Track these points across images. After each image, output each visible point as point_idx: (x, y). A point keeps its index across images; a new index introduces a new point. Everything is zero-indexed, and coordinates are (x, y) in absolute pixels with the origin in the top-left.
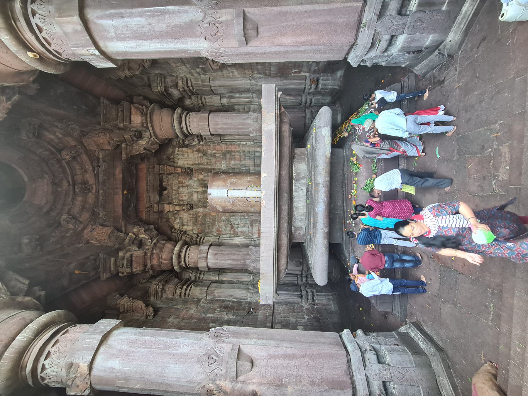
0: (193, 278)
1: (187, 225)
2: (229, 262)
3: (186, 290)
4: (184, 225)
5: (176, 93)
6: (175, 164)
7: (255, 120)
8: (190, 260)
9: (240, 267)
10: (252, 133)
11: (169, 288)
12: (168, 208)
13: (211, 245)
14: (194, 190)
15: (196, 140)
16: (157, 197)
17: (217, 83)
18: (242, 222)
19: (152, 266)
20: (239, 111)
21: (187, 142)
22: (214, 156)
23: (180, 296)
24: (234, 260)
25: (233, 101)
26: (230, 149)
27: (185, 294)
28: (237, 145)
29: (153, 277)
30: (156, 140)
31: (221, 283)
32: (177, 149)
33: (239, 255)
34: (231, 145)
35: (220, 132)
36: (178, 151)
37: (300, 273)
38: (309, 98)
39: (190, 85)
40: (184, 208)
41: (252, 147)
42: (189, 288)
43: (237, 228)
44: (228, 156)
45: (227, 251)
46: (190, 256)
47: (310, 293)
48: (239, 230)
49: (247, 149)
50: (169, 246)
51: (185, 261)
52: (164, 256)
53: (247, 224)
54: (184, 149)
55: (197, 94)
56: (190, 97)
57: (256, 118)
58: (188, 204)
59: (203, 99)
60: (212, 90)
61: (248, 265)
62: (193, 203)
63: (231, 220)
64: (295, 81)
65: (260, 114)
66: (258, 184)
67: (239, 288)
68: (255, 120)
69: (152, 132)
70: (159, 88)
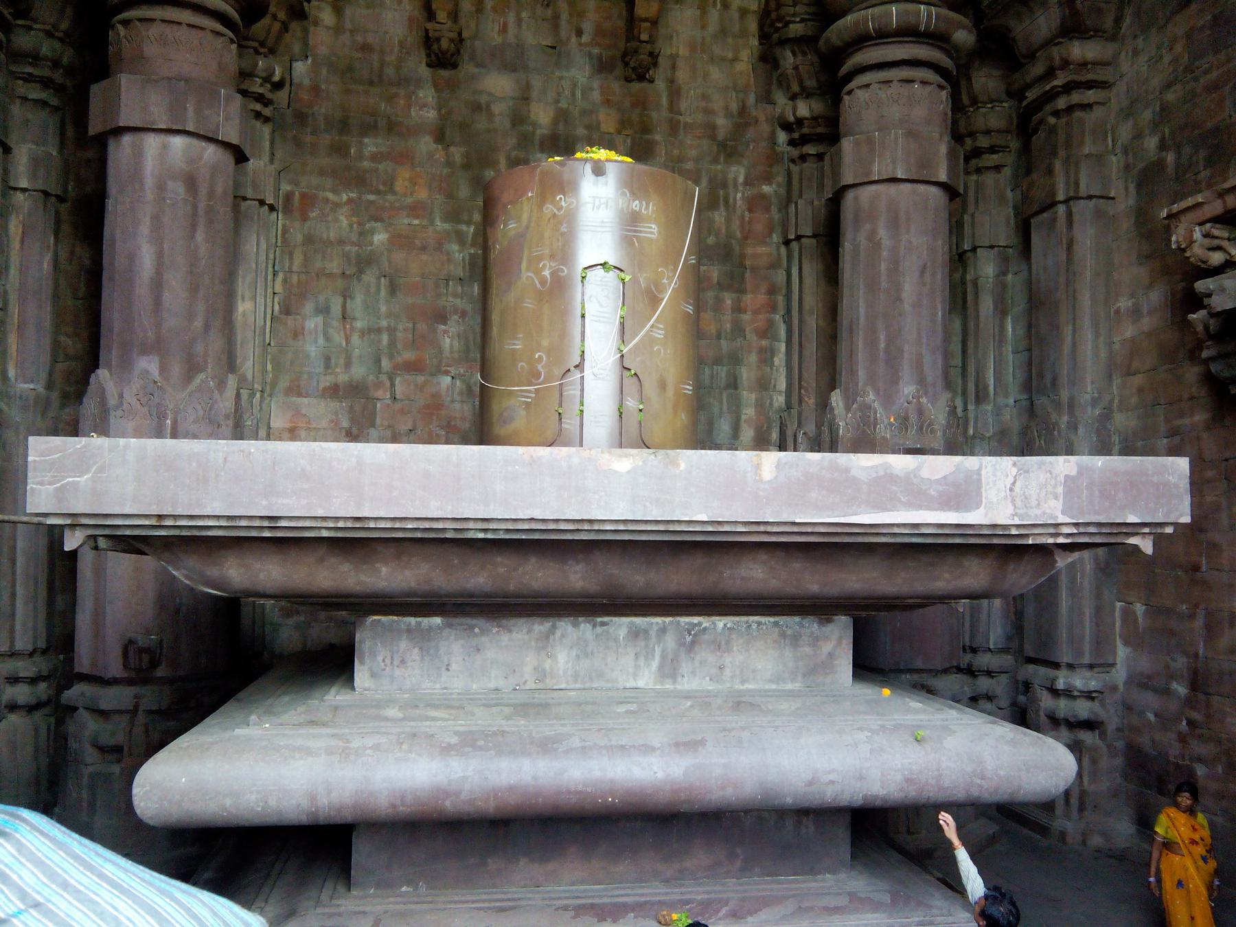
1: (338, 30)
7: (913, 418)
8: (155, 30)
13: (240, 156)
14: (537, 82)
18: (355, 339)
21: (788, 59)
24: (158, 284)
26: (749, 286)
28: (771, 324)
33: (191, 316)
34: (772, 291)
40: (442, 16)
41: (760, 405)
43: (324, 310)
46: (183, 33)
48: (313, 323)
49: (747, 374)
53: (348, 365)
57: (924, 426)
58: (461, 40)
59: (994, 159)
60: (1054, 204)
61: (126, 364)
62: (467, 68)
63: (369, 277)
64: (1088, 612)
65: (938, 443)
66: (632, 435)
68: (913, 418)
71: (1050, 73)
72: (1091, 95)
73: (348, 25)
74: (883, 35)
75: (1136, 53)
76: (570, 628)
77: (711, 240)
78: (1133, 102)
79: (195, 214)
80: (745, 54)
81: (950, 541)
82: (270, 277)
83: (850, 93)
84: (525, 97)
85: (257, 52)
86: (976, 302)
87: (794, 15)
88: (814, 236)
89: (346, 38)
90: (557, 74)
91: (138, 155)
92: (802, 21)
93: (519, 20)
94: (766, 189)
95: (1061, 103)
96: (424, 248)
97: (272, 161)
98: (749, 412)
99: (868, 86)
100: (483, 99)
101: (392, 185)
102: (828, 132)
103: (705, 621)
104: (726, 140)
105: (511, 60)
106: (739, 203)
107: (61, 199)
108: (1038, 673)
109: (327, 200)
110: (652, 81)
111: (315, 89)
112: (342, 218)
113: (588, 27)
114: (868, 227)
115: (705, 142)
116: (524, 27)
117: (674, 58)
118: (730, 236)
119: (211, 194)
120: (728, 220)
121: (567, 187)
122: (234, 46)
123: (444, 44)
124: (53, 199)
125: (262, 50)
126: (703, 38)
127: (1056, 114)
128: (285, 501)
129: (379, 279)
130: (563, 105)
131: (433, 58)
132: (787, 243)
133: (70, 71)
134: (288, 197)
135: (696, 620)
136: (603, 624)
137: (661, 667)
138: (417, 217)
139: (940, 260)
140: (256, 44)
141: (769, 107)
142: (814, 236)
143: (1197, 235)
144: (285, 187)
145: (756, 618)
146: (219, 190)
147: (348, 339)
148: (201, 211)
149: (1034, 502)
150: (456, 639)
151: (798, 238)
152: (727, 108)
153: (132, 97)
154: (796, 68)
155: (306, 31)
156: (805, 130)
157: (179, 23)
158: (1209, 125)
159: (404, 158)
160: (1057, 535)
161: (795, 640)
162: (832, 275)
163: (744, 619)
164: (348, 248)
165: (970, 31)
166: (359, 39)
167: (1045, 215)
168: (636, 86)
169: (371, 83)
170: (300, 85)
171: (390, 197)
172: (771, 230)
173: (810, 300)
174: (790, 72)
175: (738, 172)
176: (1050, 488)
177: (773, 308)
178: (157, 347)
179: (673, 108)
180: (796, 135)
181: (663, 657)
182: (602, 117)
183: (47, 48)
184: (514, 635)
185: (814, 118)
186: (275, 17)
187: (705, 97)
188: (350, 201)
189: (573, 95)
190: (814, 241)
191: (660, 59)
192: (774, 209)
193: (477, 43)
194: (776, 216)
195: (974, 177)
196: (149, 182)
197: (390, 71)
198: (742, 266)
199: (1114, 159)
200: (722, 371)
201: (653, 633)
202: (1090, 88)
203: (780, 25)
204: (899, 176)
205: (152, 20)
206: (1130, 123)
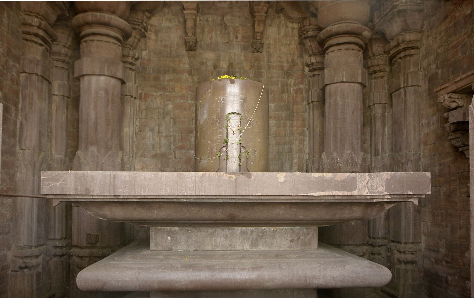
1: (156, 41)
2: (93, 115)
3: (36, 35)
4: (156, 33)
6: (268, 22)
10: (328, 157)
13: (123, 82)
15: (313, 60)
17: (411, 99)
22: (284, 88)
23: (25, 24)
24: (96, 124)
27: (28, 33)
31: (49, 100)
32: (296, 26)
36: (293, 28)
39: (407, 52)
40: (190, 34)
42: (40, 41)
44: (284, 114)
51: (94, 34)
54: (297, 38)
58: (197, 42)
60: (400, 89)
62: (199, 51)
67: (40, 134)
71: (398, 45)
72: (412, 51)
73: (160, 39)
74: (338, 34)
75: (428, 36)
76: (221, 231)
77: (282, 104)
78: (427, 53)
79: (108, 101)
80: (293, 42)
81: (346, 201)
82: (135, 120)
84: (218, 59)
85: (130, 49)
86: (375, 122)
87: (309, 29)
88: (318, 101)
90: (229, 51)
91: (90, 83)
92: (312, 31)
93: (216, 35)
94: (301, 86)
96: (185, 109)
97: (135, 83)
100: (204, 61)
101: (174, 90)
102: (320, 68)
103: (266, 228)
104: (287, 71)
105: (213, 47)
106: (292, 91)
107: (69, 98)
109: (153, 95)
110: (261, 52)
111: (149, 60)
113: (240, 36)
114: (334, 98)
115: (280, 72)
116: (218, 36)
117: (269, 44)
118: (289, 102)
119: (113, 95)
120: (288, 97)
121: (223, 89)
122: (120, 48)
123: (191, 43)
124: (66, 98)
126: (279, 38)
127: (400, 58)
129: (170, 120)
130: (231, 61)
131: (188, 48)
132: (309, 104)
133: (71, 57)
134: (141, 95)
135: (263, 228)
136: (232, 229)
138: (182, 99)
139: (359, 108)
140: (130, 46)
141: (302, 59)
142: (318, 101)
143: (447, 97)
144: (140, 91)
145: (284, 227)
146: (116, 93)
148: (110, 100)
149: (375, 188)
151: (312, 102)
152: (287, 60)
153: (86, 65)
154: (311, 46)
155: (146, 41)
156: (314, 67)
158: (453, 60)
159: (178, 80)
162: (323, 114)
163: (280, 228)
164: (160, 110)
165: (369, 32)
166: (163, 43)
167: (397, 92)
168: (256, 54)
169: (167, 57)
170: (144, 59)
171: (174, 93)
172: (303, 100)
173: (316, 123)
174: (308, 48)
180: (311, 68)
181: (252, 240)
182: (244, 65)
183: (63, 51)
184: (202, 233)
185: (318, 63)
186: (135, 37)
187: (279, 57)
188: (161, 95)
189: (235, 58)
190: (318, 103)
191: (264, 45)
192: (304, 93)
193: (202, 43)
194: (305, 95)
195: (374, 80)
196: (93, 92)
197: (174, 53)
198: (293, 112)
199: (421, 73)
201: (249, 232)
202: (412, 49)
203: (305, 32)
204: (344, 81)
206: (426, 60)
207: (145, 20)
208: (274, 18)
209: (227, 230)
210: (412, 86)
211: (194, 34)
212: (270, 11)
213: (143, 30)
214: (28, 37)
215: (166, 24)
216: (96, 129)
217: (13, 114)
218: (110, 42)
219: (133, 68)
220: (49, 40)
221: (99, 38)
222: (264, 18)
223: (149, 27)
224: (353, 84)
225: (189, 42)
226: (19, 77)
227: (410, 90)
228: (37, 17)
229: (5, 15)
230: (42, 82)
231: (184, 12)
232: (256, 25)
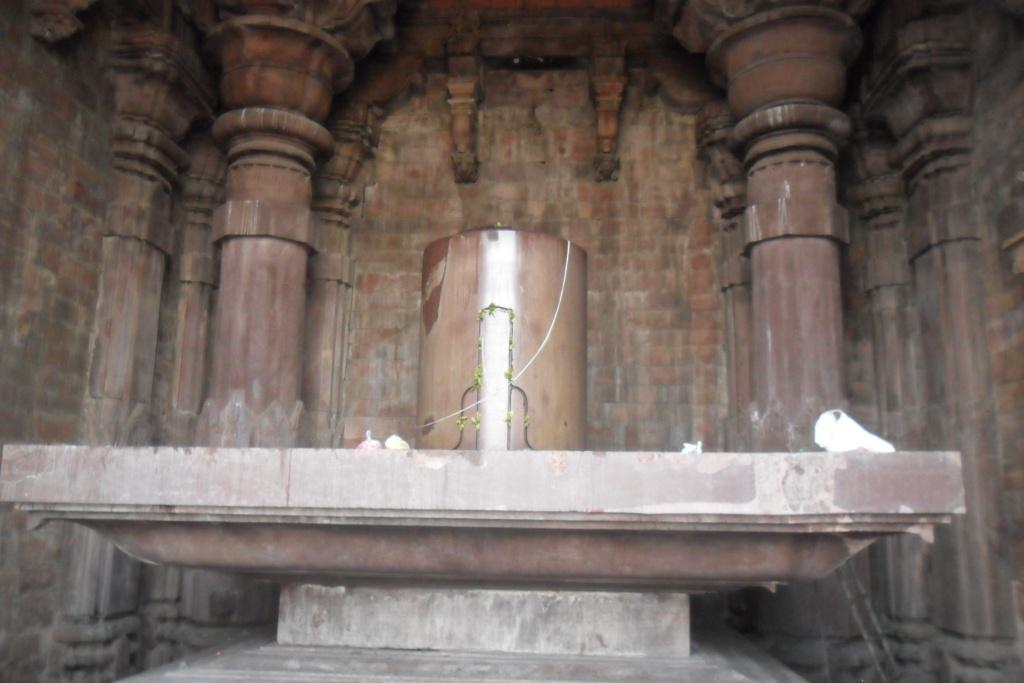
0: (191, 187)
1: (396, 163)
2: (240, 323)
3: (143, 159)
4: (396, 149)
5: (907, 109)
6: (629, 114)
8: (252, 172)
9: (219, 363)
11: (154, 98)
12: (461, 88)
13: (311, 252)
15: (729, 191)
16: (505, 49)
17: (958, 269)
18: (404, 375)
19: (235, 34)
20: (847, 359)
22: (668, 258)
24: (246, 340)
25: (892, 333)
27: (127, 156)
29: (200, 38)
30: (718, 41)
32: (690, 120)
34: (714, 327)
35: (761, 283)
36: (684, 126)
37: (187, 611)
38: (924, 653)
39: (941, 163)
40: (462, 147)
42: (150, 171)
43: (383, 355)
44: (668, 315)
45: (286, 314)
47: (99, 653)
48: (375, 363)
49: (695, 392)
50: (313, 92)
52: (273, 77)
53: (398, 393)
54: (693, 146)
55: (908, 192)
56: (895, 165)
58: (477, 163)
60: (929, 248)
62: (483, 181)
67: (137, 364)
69: (750, 22)
70: (921, 47)
76: (446, 599)
77: (664, 291)
83: (752, 173)
84: (523, 198)
85: (341, 183)
89: (401, 168)
91: (238, 253)
92: (725, 127)
93: (519, 146)
95: (930, 168)
98: (698, 422)
99: (763, 168)
105: (514, 174)
108: (949, 644)
109: (386, 279)
110: (616, 180)
111: (380, 204)
112: (396, 290)
113: (568, 147)
120: (677, 276)
123: (464, 166)
125: (346, 181)
128: (176, 493)
130: (552, 201)
132: (724, 290)
135: (550, 594)
136: (473, 596)
137: (521, 634)
144: (358, 271)
147: (398, 374)
150: (356, 605)
154: (723, 161)
157: (268, 165)
160: (836, 524)
161: (638, 614)
162: (750, 313)
163: (593, 594)
166: (410, 168)
168: (605, 185)
172: (711, 282)
175: (684, 240)
176: (821, 482)
177: (714, 340)
178: (244, 383)
179: (633, 198)
180: (726, 210)
187: (656, 188)
188: (402, 278)
193: (490, 165)
194: (715, 270)
200: (676, 390)
201: (515, 604)
203: (707, 132)
204: (791, 233)
205: (252, 165)
207: (370, 123)
208: (641, 106)
209: (462, 597)
210: (960, 239)
211: (473, 147)
212: (633, 92)
213: (366, 143)
214: (127, 163)
215: (415, 128)
216: (246, 352)
217: (82, 322)
218: (283, 168)
219: (346, 221)
220: (171, 169)
221: (263, 159)
222: (616, 106)
223: (382, 137)
224: (812, 241)
225: (459, 164)
226: (100, 243)
227: (955, 250)
228: (146, 123)
229: (79, 120)
230: (149, 255)
231: (450, 101)
232: (601, 121)
